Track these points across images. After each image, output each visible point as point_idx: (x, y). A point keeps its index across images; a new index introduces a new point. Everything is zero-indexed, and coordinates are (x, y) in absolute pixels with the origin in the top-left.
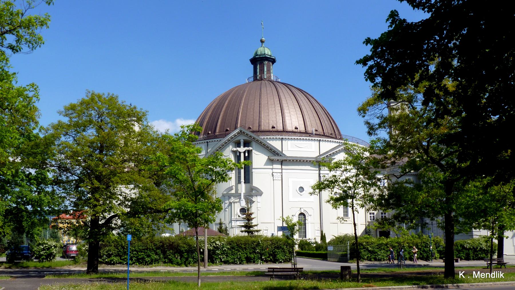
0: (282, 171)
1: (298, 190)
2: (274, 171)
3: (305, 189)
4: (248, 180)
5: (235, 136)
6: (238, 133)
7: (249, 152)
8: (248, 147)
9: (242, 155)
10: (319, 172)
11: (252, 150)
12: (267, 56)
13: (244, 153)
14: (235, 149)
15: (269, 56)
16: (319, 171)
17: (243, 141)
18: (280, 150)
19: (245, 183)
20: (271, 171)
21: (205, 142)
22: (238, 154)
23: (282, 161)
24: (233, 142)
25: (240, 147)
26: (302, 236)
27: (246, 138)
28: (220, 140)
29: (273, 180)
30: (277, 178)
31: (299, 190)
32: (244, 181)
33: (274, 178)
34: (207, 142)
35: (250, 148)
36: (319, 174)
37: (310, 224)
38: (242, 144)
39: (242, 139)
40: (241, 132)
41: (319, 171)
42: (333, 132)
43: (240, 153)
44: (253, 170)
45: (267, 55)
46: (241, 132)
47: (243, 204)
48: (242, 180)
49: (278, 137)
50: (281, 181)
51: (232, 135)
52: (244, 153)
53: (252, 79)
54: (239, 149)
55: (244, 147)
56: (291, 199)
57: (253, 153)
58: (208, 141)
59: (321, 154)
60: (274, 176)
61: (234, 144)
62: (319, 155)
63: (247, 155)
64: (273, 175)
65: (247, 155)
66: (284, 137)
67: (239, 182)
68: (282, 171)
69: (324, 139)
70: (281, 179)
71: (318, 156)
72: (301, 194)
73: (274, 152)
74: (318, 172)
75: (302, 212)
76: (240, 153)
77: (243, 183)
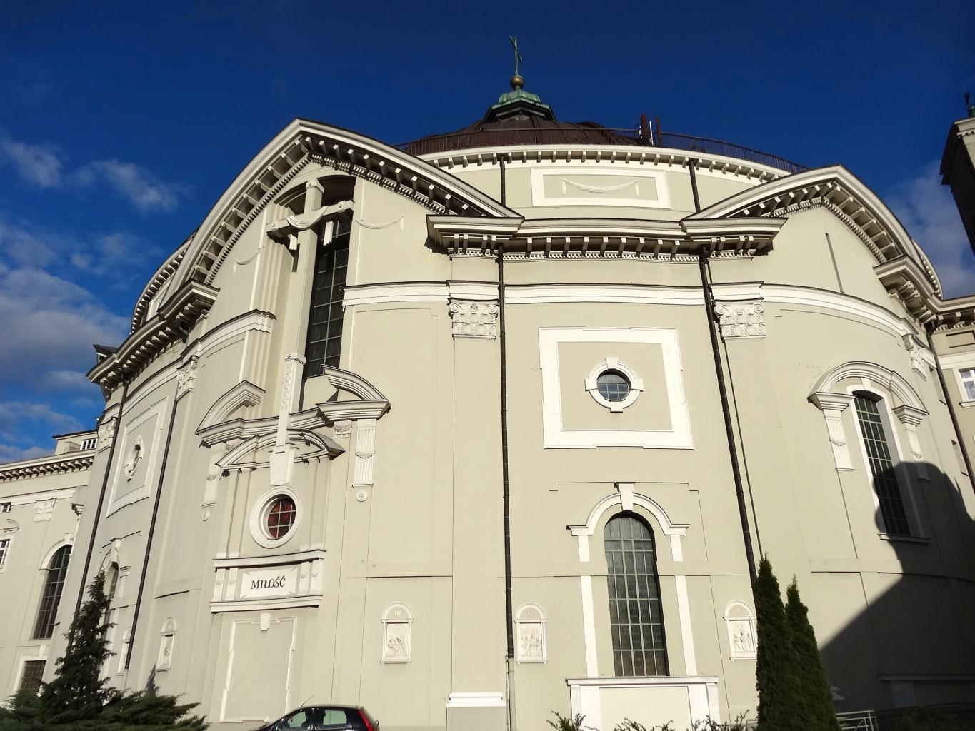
1: (592, 383)
2: (457, 291)
3: (636, 383)
6: (297, 154)
12: (523, 99)
15: (529, 102)
16: (707, 289)
17: (315, 183)
24: (276, 202)
26: (639, 664)
31: (602, 388)
36: (710, 305)
39: (312, 174)
41: (707, 289)
56: (555, 434)
63: (328, 239)
70: (496, 332)
72: (616, 406)
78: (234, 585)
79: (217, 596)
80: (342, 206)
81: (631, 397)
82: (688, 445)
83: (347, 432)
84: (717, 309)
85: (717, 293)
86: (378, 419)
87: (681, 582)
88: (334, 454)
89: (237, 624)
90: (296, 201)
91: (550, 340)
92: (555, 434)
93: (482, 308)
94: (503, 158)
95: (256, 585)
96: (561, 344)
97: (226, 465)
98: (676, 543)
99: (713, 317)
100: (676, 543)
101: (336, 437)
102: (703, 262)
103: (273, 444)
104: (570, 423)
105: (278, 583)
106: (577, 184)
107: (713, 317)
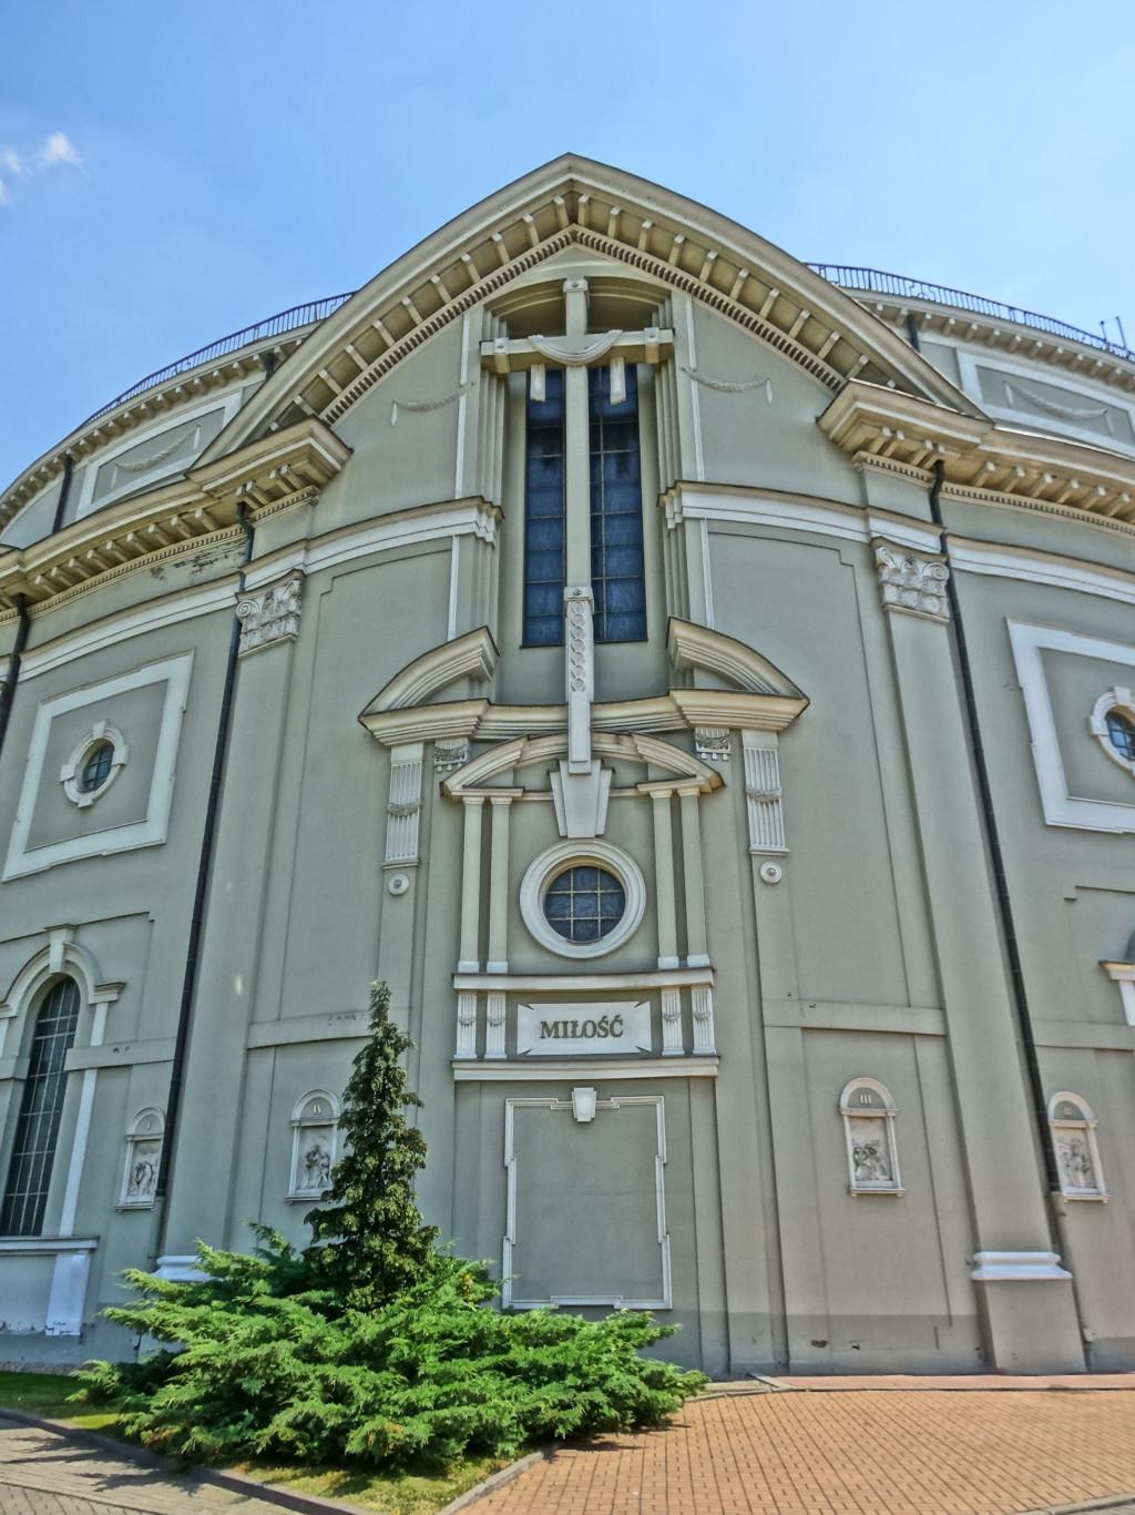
14: (503, 347)
17: (583, 284)
20: (850, 528)
27: (609, 267)
29: (884, 610)
30: (911, 599)
33: (891, 595)
43: (556, 374)
52: (598, 373)
57: (679, 374)
60: (885, 573)
63: (618, 388)
64: (875, 567)
67: (544, 628)
77: (579, 619)
78: (502, 1029)
79: (466, 1045)
80: (651, 337)
83: (724, 750)
86: (778, 733)
89: (515, 1108)
91: (1025, 637)
93: (924, 570)
95: (548, 1030)
97: (459, 787)
103: (564, 755)
105: (606, 1028)
106: (1028, 393)
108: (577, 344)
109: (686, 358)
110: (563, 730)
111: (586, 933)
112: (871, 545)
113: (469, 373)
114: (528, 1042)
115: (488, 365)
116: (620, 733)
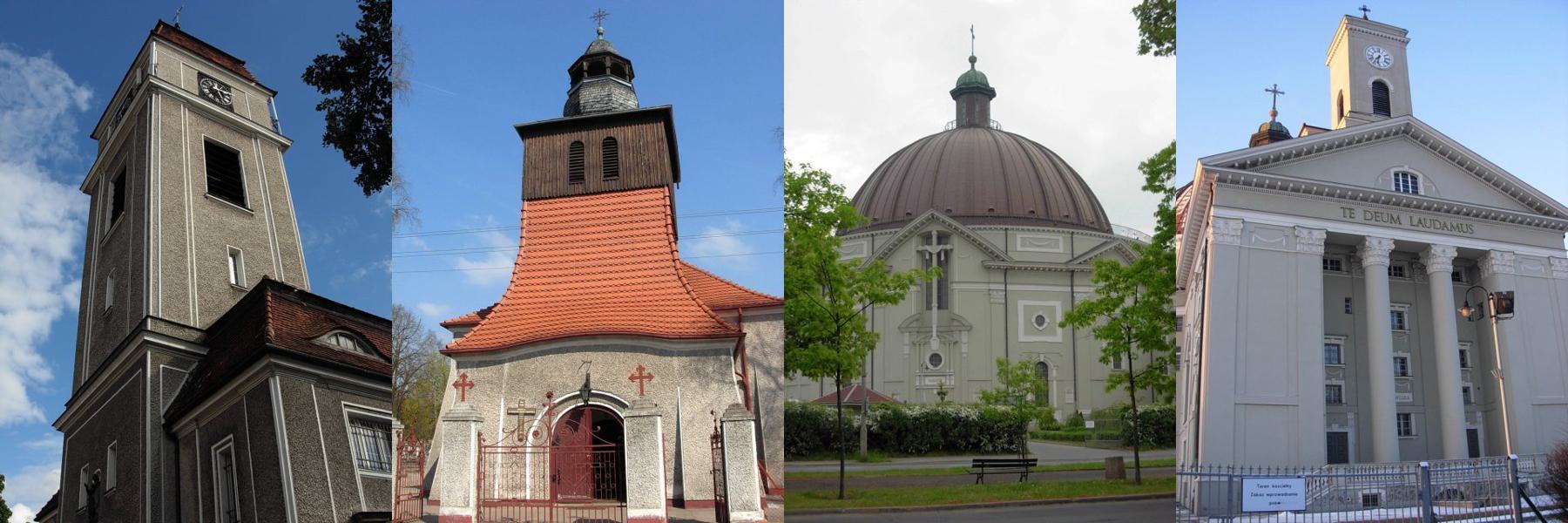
0: (1006, 287)
1: (1033, 320)
2: (993, 286)
3: (1047, 320)
4: (943, 304)
5: (922, 224)
6: (928, 220)
7: (947, 253)
8: (946, 244)
9: (935, 258)
10: (1072, 289)
11: (952, 250)
13: (939, 254)
14: (920, 248)
16: (1072, 286)
17: (936, 233)
18: (1003, 249)
19: (939, 308)
20: (985, 287)
21: (868, 236)
22: (927, 257)
23: (1006, 269)
25: (930, 244)
27: (941, 228)
28: (896, 232)
32: (936, 305)
34: (872, 235)
35: (948, 247)
36: (1073, 293)
37: (1055, 382)
38: (934, 239)
39: (934, 230)
40: (933, 217)
41: (1072, 286)
42: (1095, 220)
44: (955, 286)
45: (980, 84)
46: (933, 217)
47: (935, 345)
48: (935, 304)
49: (999, 227)
50: (1002, 307)
51: (914, 223)
52: (939, 254)
53: (955, 125)
54: (927, 247)
55: (939, 243)
56: (1022, 338)
58: (874, 232)
59: (1075, 256)
61: (920, 239)
62: (1070, 258)
63: (943, 258)
65: (943, 258)
66: (1009, 227)
67: (929, 308)
68: (1006, 287)
69: (1080, 231)
70: (1004, 301)
71: (1071, 261)
72: (1041, 328)
73: (992, 253)
74: (1069, 289)
75: (1042, 360)
76: (931, 254)
77: (935, 309)
81: (1045, 325)
82: (1061, 341)
84: (1075, 295)
85: (1075, 289)
87: (1055, 382)
88: (955, 343)
90: (927, 238)
91: (1021, 304)
92: (1022, 338)
93: (1000, 293)
94: (1006, 229)
96: (1025, 306)
98: (1055, 371)
99: (1073, 297)
100: (1055, 371)
101: (956, 337)
102: (1072, 276)
103: (932, 336)
104: (1027, 333)
107: (1073, 297)
108: (935, 248)
109: (955, 251)
110: (932, 332)
111: (936, 366)
112: (990, 290)
113: (914, 253)
114: (927, 382)
115: (918, 251)
116: (941, 332)
